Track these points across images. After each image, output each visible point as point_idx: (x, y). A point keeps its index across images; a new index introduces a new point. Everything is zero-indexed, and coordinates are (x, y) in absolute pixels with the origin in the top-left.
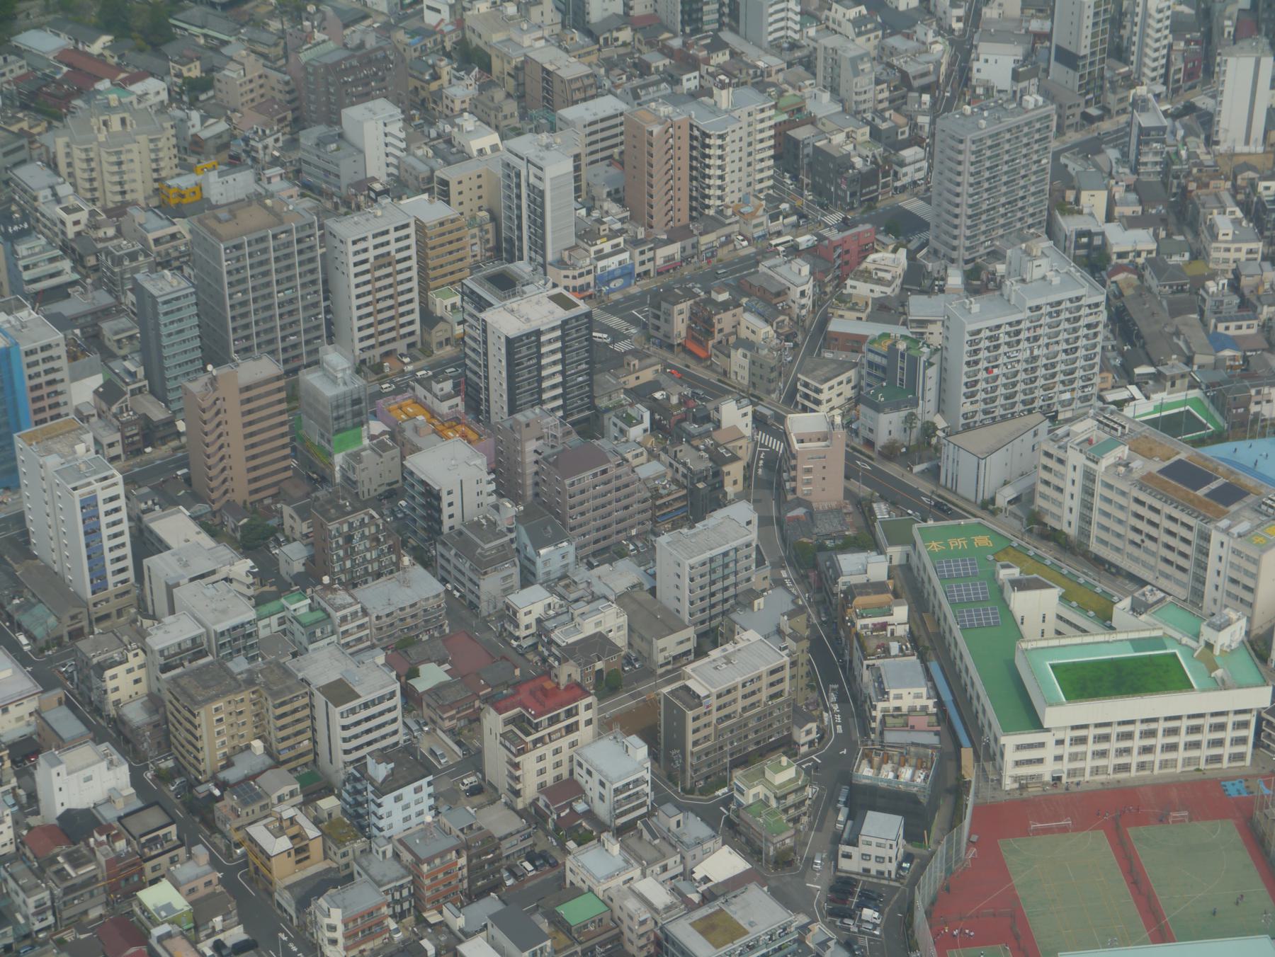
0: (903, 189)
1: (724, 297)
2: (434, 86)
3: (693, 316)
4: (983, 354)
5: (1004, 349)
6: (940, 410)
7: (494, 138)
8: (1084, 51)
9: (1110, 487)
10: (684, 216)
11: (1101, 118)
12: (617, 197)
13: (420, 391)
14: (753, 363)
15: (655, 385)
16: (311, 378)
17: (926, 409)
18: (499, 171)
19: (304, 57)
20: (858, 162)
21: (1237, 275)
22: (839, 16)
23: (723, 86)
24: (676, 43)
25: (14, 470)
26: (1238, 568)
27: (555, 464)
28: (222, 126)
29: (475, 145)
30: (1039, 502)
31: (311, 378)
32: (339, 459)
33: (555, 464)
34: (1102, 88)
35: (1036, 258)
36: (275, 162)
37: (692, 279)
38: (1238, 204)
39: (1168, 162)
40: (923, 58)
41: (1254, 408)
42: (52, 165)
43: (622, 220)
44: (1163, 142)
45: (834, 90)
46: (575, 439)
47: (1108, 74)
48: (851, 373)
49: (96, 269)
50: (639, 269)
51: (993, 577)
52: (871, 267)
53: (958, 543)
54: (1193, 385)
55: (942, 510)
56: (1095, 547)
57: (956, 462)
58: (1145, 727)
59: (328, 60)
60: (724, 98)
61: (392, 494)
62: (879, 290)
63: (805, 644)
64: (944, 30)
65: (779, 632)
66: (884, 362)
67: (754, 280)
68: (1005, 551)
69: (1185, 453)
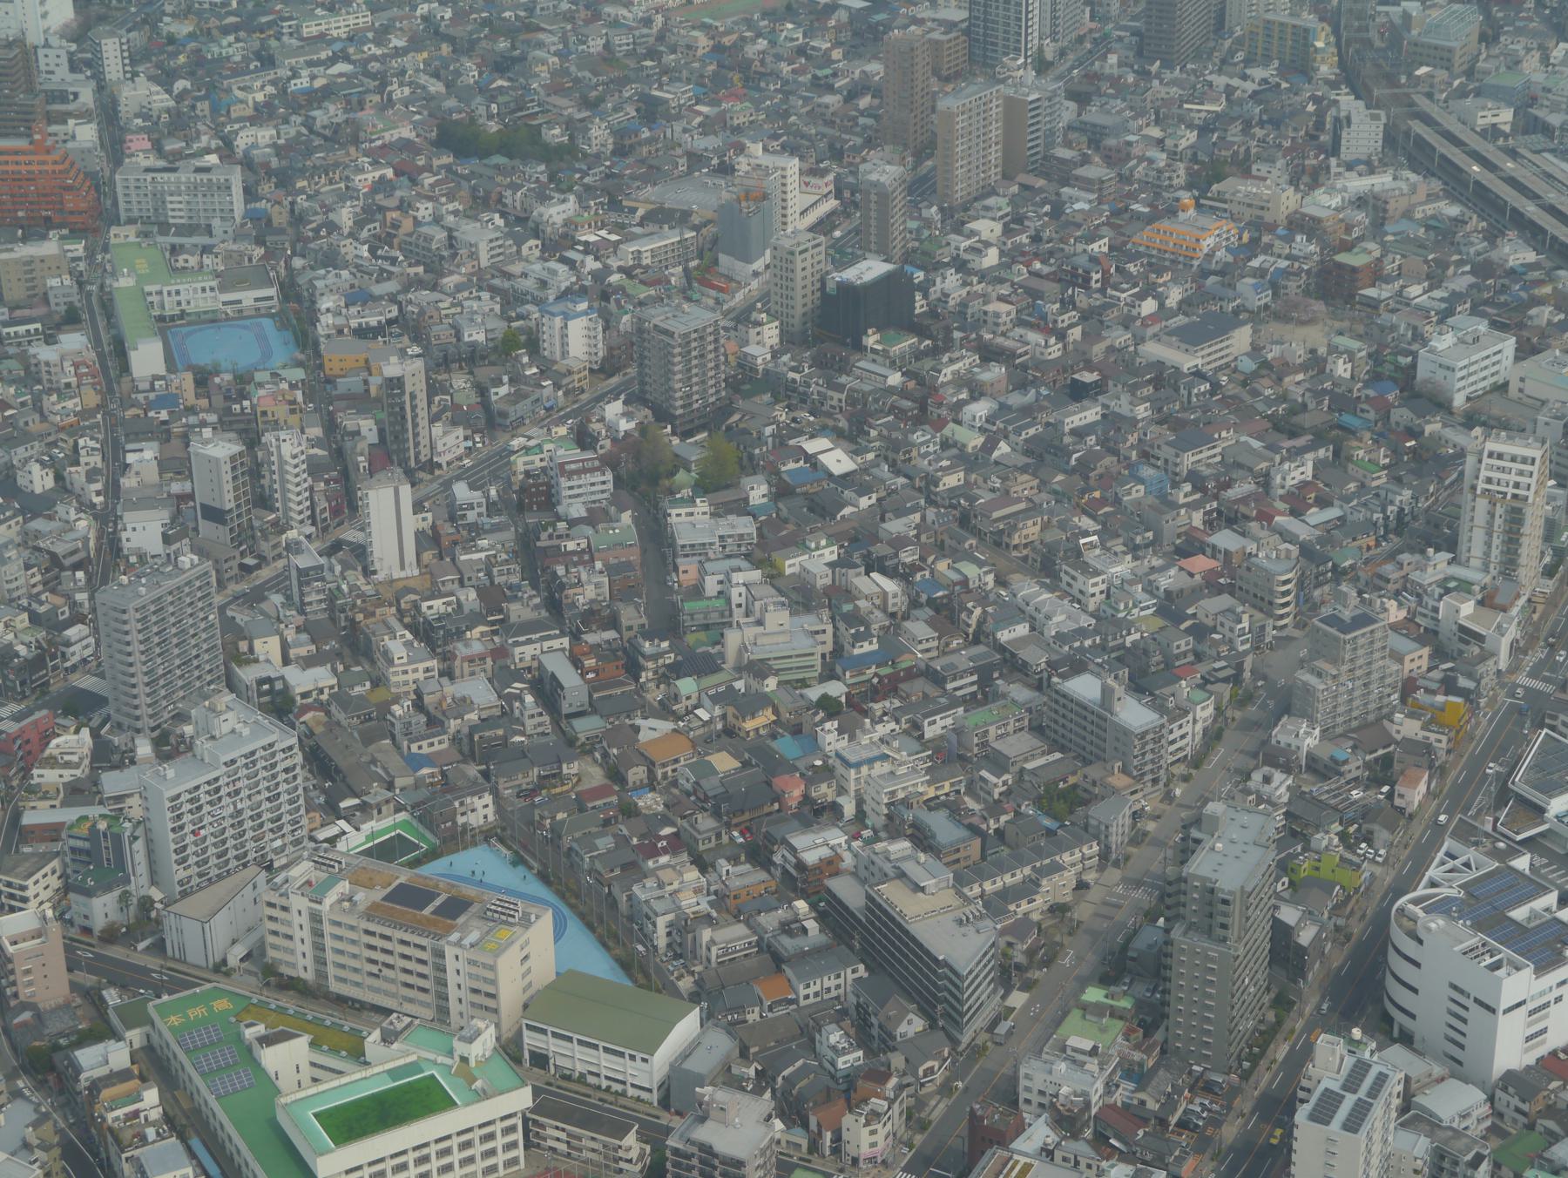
0: (74, 668)
4: (187, 818)
5: (207, 808)
6: (153, 882)
9: (338, 924)
11: (258, 567)
17: (140, 884)
21: (419, 694)
26: (477, 978)
30: (272, 954)
34: (253, 537)
35: (220, 713)
38: (406, 627)
39: (331, 598)
40: (70, 536)
41: (461, 820)
44: (323, 579)
47: (256, 524)
48: (55, 863)
51: (239, 1037)
52: (56, 752)
53: (197, 1012)
54: (398, 809)
55: (175, 985)
56: (335, 987)
57: (180, 931)
58: (417, 1154)
62: (68, 775)
63: (57, 1152)
64: (85, 506)
65: (26, 1146)
66: (87, 845)
68: (246, 1010)
69: (404, 877)
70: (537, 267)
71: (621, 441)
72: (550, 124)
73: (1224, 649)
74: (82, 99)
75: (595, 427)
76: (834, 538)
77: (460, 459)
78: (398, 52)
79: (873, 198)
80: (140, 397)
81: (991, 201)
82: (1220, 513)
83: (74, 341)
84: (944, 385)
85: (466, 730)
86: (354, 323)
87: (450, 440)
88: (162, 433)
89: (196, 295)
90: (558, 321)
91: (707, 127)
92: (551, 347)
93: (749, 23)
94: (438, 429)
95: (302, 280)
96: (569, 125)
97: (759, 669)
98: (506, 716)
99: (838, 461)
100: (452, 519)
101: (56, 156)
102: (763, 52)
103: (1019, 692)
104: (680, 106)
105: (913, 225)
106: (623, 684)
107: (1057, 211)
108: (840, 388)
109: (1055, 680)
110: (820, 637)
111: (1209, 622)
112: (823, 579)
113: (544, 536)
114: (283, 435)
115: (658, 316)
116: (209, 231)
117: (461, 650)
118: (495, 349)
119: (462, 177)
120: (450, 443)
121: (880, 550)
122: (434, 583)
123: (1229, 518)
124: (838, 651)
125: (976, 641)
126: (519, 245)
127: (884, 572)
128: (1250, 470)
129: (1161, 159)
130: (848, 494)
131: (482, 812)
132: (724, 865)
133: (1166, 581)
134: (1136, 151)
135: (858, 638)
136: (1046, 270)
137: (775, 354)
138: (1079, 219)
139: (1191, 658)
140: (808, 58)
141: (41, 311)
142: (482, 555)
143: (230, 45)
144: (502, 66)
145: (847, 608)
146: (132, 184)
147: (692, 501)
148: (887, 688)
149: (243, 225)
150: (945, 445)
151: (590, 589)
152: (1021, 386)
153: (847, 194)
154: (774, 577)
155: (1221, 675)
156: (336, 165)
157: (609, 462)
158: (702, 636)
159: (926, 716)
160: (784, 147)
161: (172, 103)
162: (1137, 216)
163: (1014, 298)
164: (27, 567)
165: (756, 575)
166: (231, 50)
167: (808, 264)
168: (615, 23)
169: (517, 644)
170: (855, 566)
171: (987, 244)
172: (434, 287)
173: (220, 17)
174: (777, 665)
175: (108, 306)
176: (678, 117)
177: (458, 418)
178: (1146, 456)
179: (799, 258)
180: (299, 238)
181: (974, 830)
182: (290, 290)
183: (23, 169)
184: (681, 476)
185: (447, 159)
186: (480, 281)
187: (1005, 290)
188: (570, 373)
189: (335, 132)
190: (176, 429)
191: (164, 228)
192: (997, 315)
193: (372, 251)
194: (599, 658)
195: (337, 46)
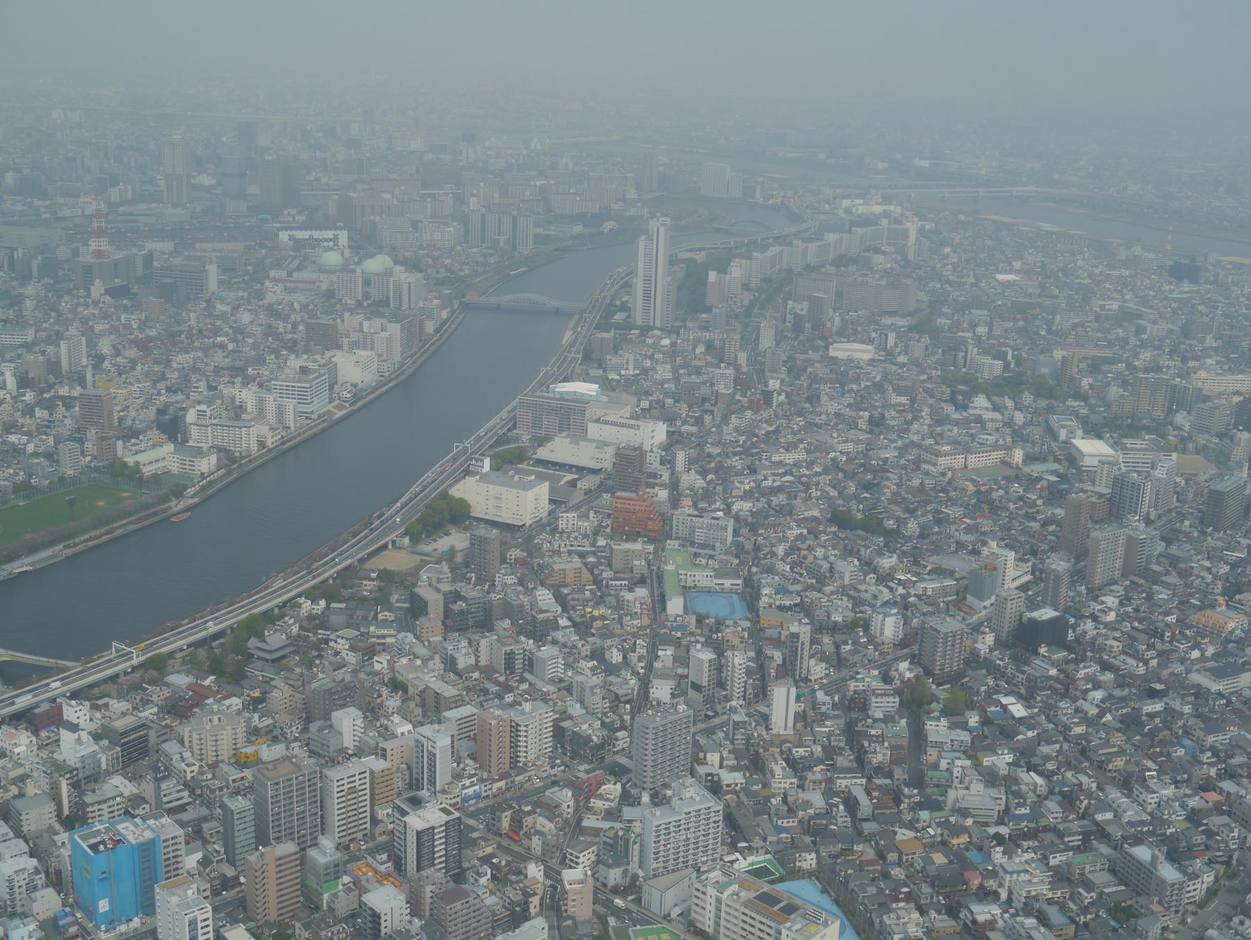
1: (528, 808)
2: (379, 700)
3: (512, 819)
4: (662, 837)
5: (673, 834)
6: (640, 867)
7: (410, 727)
8: (705, 684)
9: (729, 906)
10: (507, 766)
12: (473, 757)
13: (370, 860)
14: (543, 843)
15: (493, 855)
16: (313, 853)
17: (634, 866)
18: (413, 744)
19: (313, 686)
20: (595, 738)
22: (583, 666)
23: (527, 700)
24: (502, 679)
25: (153, 904)
27: (442, 898)
28: (270, 721)
29: (399, 730)
30: (693, 915)
31: (313, 853)
32: (326, 896)
33: (442, 898)
36: (296, 739)
37: (512, 799)
38: (784, 759)
39: (748, 738)
40: (625, 687)
41: (798, 864)
42: (182, 742)
43: (475, 769)
44: (745, 728)
45: (582, 703)
46: (452, 884)
47: (716, 695)
48: (595, 848)
49: (201, 796)
50: (484, 794)
52: (603, 792)
54: (767, 852)
59: (326, 687)
60: (527, 706)
61: (353, 916)
64: (637, 674)
67: (543, 799)
69: (766, 888)
70: (873, 588)
71: (906, 683)
73: (1222, 846)
75: (893, 673)
76: (1012, 750)
77: (821, 679)
78: (817, 474)
79: (1052, 577)
80: (669, 624)
81: (1114, 587)
82: (1226, 771)
83: (642, 592)
84: (1079, 679)
85: (807, 818)
86: (778, 603)
87: (818, 668)
88: (677, 643)
89: (703, 578)
90: (881, 617)
91: (968, 530)
92: (875, 629)
93: (996, 482)
94: (813, 662)
95: (755, 578)
96: (899, 521)
97: (964, 813)
98: (828, 814)
99: (1018, 710)
100: (814, 708)
103: (1104, 849)
105: (1071, 594)
106: (891, 808)
107: (1149, 598)
108: (1023, 672)
109: (1126, 846)
110: (999, 801)
111: (1215, 829)
112: (1003, 771)
113: (860, 725)
114: (736, 653)
115: (932, 622)
116: (713, 548)
117: (810, 776)
118: (846, 626)
120: (818, 670)
121: (1035, 760)
122: (800, 740)
123: (1231, 775)
124: (1007, 810)
125: (1083, 818)
126: (865, 575)
127: (1037, 772)
128: (1245, 750)
129: (1209, 578)
130: (1022, 728)
131: (809, 862)
132: (933, 914)
133: (1194, 802)
134: (1196, 572)
135: (1019, 805)
136: (1141, 627)
137: (991, 650)
138: (1161, 603)
139: (1203, 847)
140: (1024, 502)
141: (629, 575)
142: (827, 729)
144: (867, 487)
145: (1015, 788)
146: (681, 521)
147: (938, 719)
148: (1033, 834)
150: (1077, 711)
151: (880, 755)
152: (1122, 686)
153: (1037, 573)
154: (977, 765)
155: (1220, 859)
156: (780, 524)
157: (898, 692)
158: (935, 790)
159: (1051, 853)
160: (1007, 546)
162: (1194, 606)
163: (1122, 639)
164: (604, 699)
165: (968, 763)
167: (1014, 606)
168: (927, 473)
169: (838, 778)
170: (1022, 767)
171: (1110, 609)
172: (820, 591)
174: (974, 812)
175: (660, 577)
176: (954, 523)
177: (823, 658)
178: (1187, 733)
179: (1010, 603)
180: (756, 557)
181: (1072, 920)
182: (748, 582)
183: (632, 507)
184: (934, 705)
185: (834, 529)
186: (843, 591)
187: (1117, 634)
188: (883, 644)
190: (684, 642)
191: (692, 544)
192: (1112, 647)
193: (791, 568)
194: (880, 792)
195: (788, 468)
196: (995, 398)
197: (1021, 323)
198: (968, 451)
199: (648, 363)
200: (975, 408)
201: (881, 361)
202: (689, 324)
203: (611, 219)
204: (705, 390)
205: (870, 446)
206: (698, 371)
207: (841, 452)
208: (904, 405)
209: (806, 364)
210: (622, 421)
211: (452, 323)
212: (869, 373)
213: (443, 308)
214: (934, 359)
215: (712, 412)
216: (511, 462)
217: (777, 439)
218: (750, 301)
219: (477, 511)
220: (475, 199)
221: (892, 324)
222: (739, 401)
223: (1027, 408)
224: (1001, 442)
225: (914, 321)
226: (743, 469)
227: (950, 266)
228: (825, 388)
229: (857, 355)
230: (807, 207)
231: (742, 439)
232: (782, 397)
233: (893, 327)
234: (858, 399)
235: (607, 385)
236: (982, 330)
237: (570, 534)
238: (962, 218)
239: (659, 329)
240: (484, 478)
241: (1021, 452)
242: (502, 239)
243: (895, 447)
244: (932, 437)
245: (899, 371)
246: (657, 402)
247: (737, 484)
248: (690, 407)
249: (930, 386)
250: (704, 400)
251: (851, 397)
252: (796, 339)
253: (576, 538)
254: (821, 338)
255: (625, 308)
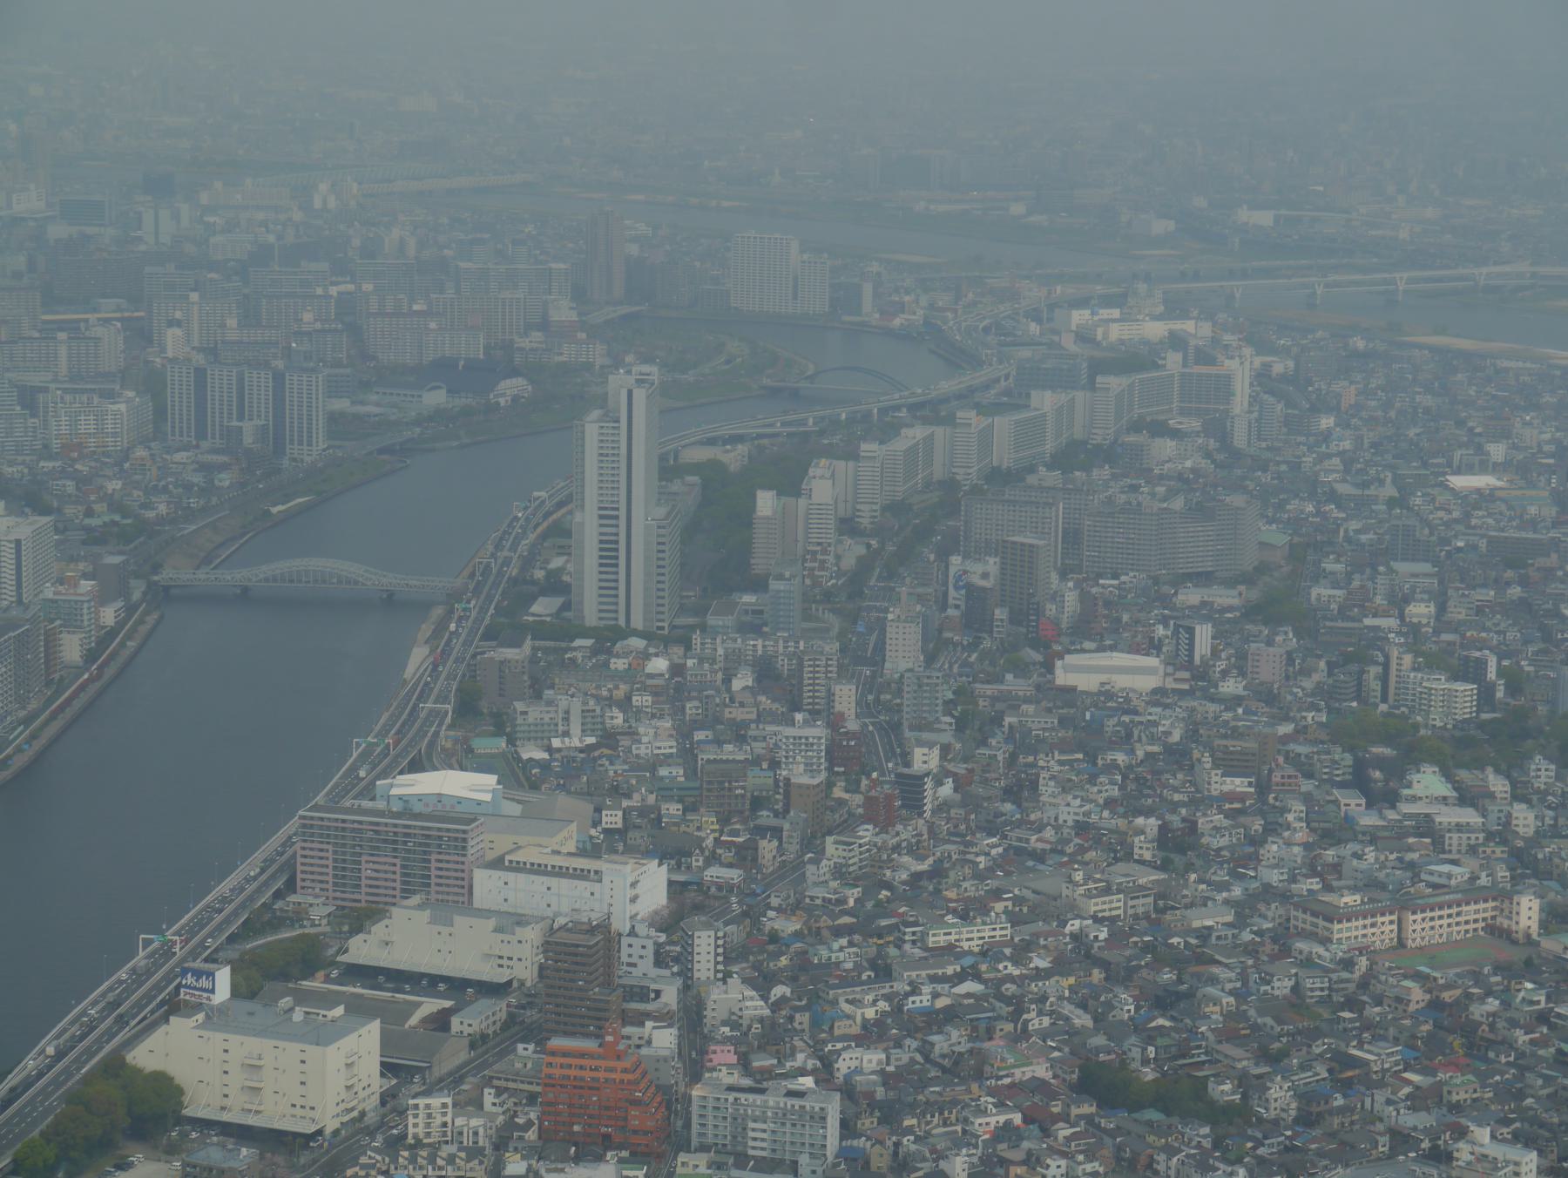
72: (1219, 1078)
74: (664, 999)
78: (1039, 974)
91: (1418, 1100)
93: (1477, 977)
96: (1245, 1082)
101: (627, 1063)
102: (1494, 1015)
104: (1384, 1071)
119: (1105, 1131)
140: (1552, 1027)
143: (841, 949)
144: (1164, 1001)
146: (711, 1104)
149: (835, 1165)
156: (954, 1103)
160: (1516, 1138)
161: (767, 1012)
166: (841, 955)
168: (1308, 963)
173: (834, 917)
176: (1381, 1084)
183: (588, 1075)
185: (1088, 1109)
189: (956, 1063)
195: (968, 961)
196: (1463, 775)
197: (1515, 591)
198: (1404, 904)
199: (617, 718)
200: (1414, 799)
201: (1182, 694)
202: (712, 620)
203: (514, 372)
204: (758, 779)
205: (1164, 899)
206: (739, 734)
207: (1097, 920)
208: (1241, 798)
209: (999, 706)
210: (558, 861)
211: (129, 637)
212: (1155, 724)
213: (102, 599)
214: (1308, 684)
215: (777, 832)
216: (285, 976)
217: (938, 891)
218: (860, 559)
219: (200, 1104)
220: (178, 332)
221: (1204, 604)
222: (841, 802)
223: (1543, 793)
224: (1484, 880)
225: (1254, 595)
226: (858, 968)
227: (1336, 461)
228: (1050, 764)
229: (1121, 681)
230: (986, 330)
231: (853, 895)
232: (947, 790)
233: (1206, 611)
234: (1131, 786)
235: (517, 776)
236: (1420, 611)
237: (435, 1148)
238: (1360, 344)
239: (644, 635)
240: (217, 1019)
241: (1536, 904)
242: (248, 428)
243: (1226, 902)
244: (1314, 873)
245: (1227, 716)
246: (643, 811)
247: (847, 1008)
248: (724, 821)
249: (1302, 749)
250: (757, 803)
251: (1113, 783)
252: (973, 646)
253: (451, 1159)
254: (1036, 644)
255: (556, 585)
